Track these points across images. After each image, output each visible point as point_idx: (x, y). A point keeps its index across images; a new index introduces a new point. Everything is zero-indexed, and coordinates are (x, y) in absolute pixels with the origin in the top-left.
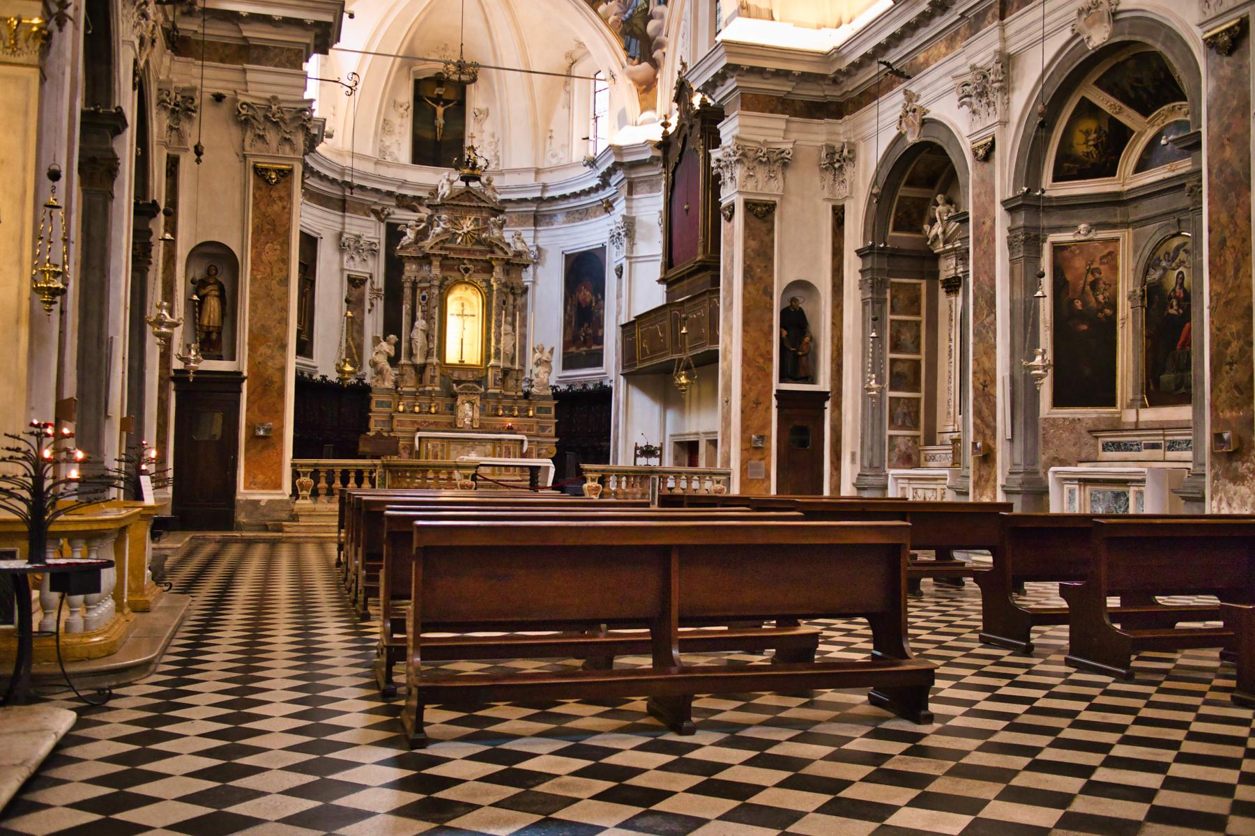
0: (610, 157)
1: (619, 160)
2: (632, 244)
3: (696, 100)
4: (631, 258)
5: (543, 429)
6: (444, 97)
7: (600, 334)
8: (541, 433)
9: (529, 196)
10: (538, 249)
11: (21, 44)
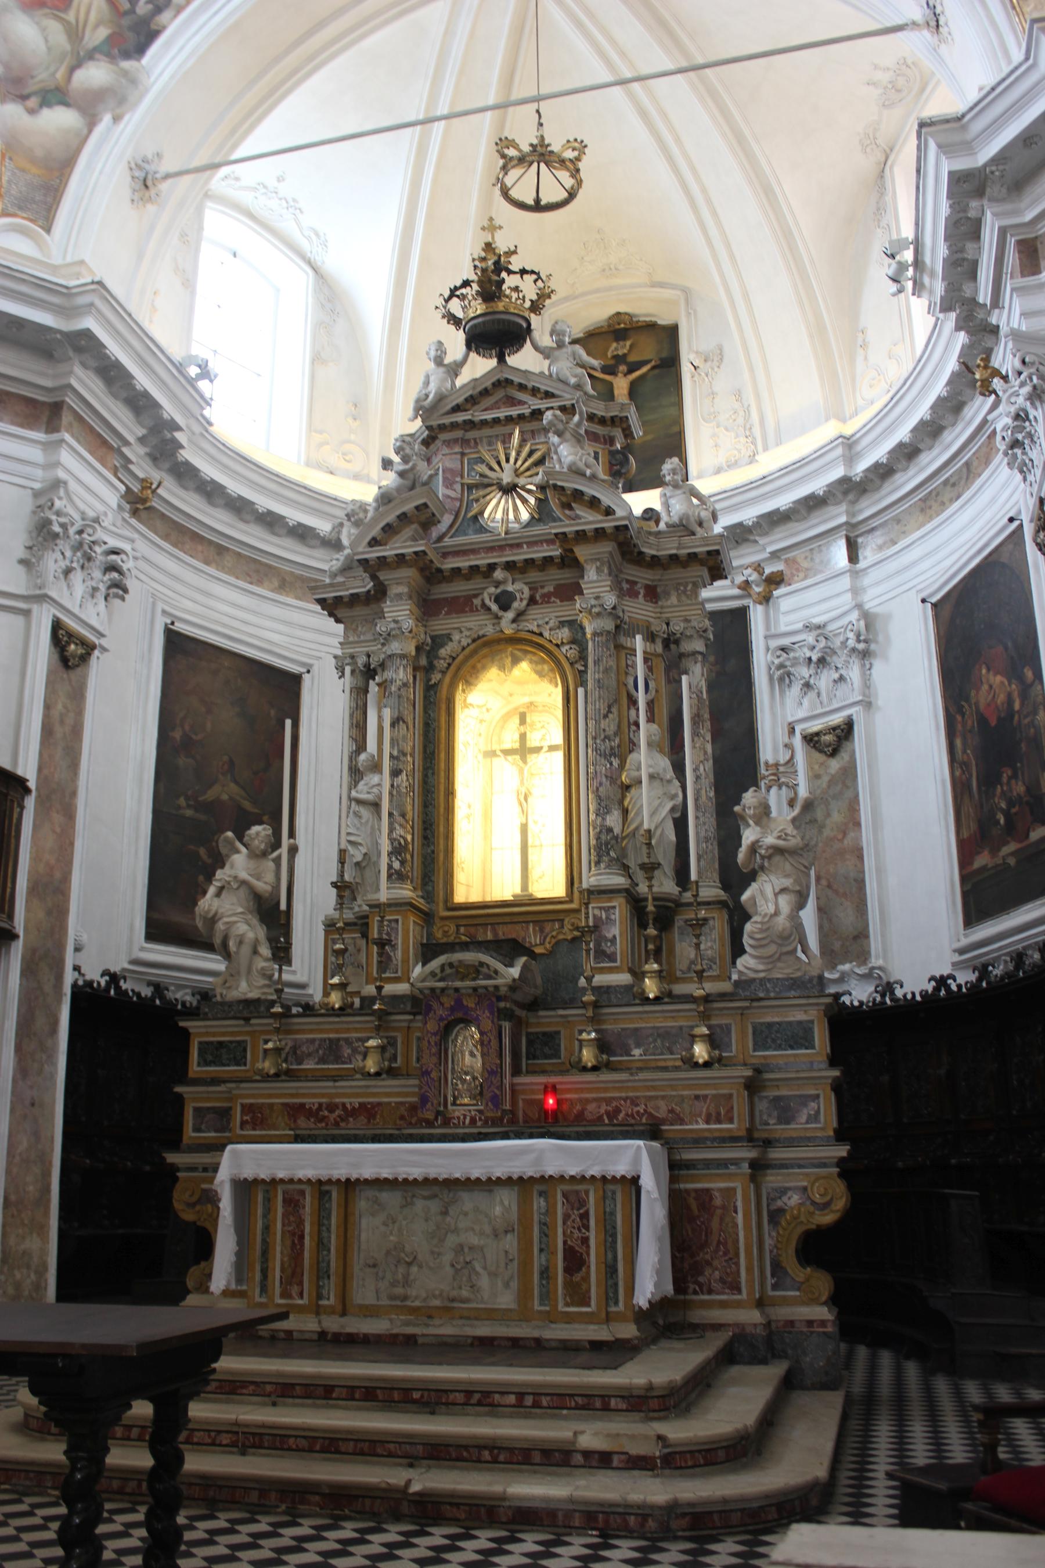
1: (963, 164)
5: (785, 1111)
6: (632, 358)
9: (817, 485)
10: (869, 619)
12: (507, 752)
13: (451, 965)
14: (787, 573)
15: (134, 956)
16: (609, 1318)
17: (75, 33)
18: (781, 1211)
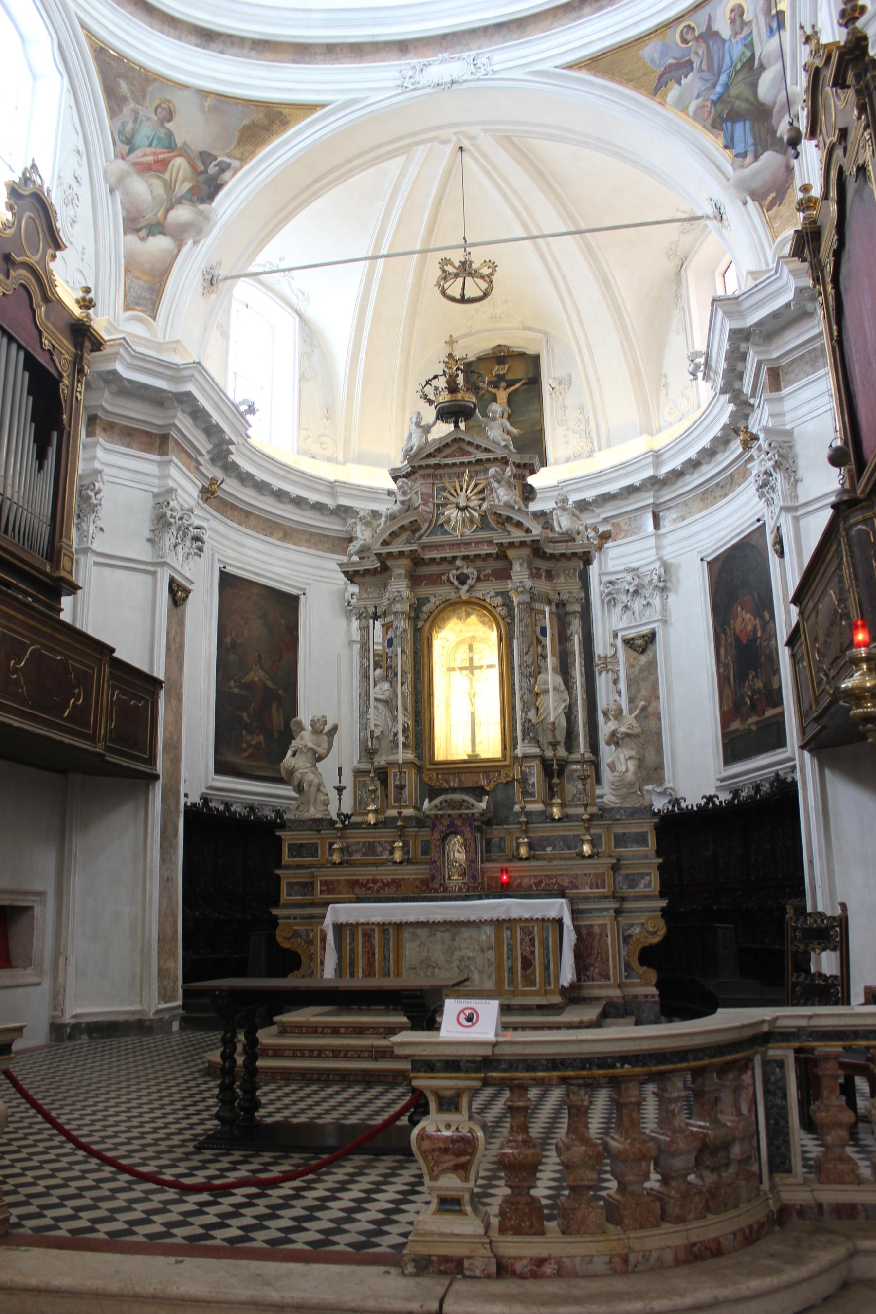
1: (738, 324)
4: (795, 509)
5: (633, 881)
6: (509, 377)
7: (776, 686)
8: (626, 891)
9: (636, 479)
10: (666, 566)
12: (461, 669)
13: (446, 801)
14: (613, 532)
15: (209, 785)
16: (546, 993)
17: (169, 187)
18: (630, 936)
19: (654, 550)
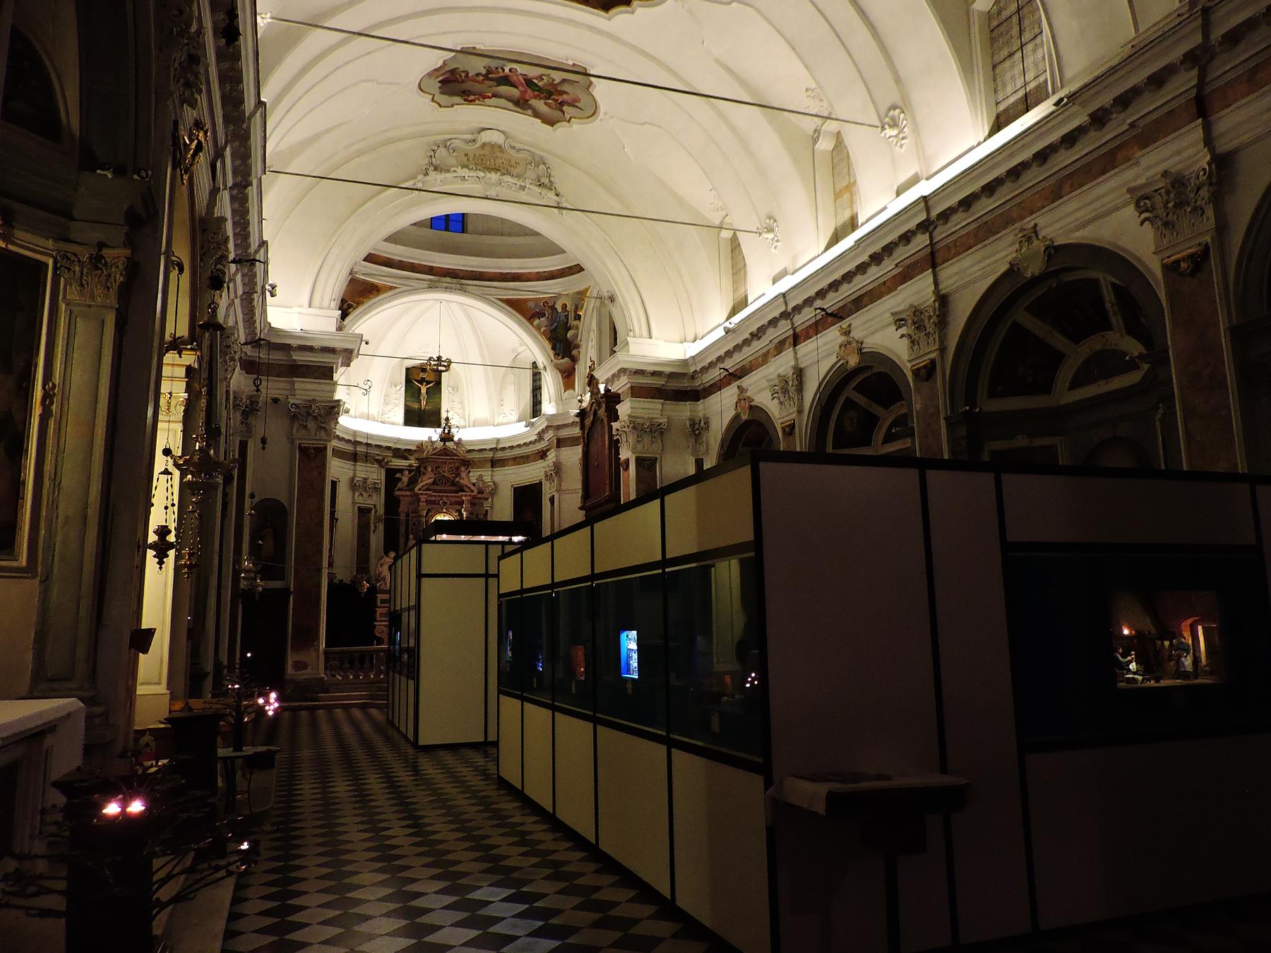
0: (543, 422)
2: (560, 480)
3: (602, 387)
10: (494, 483)
11: (172, 409)
19: (490, 477)
